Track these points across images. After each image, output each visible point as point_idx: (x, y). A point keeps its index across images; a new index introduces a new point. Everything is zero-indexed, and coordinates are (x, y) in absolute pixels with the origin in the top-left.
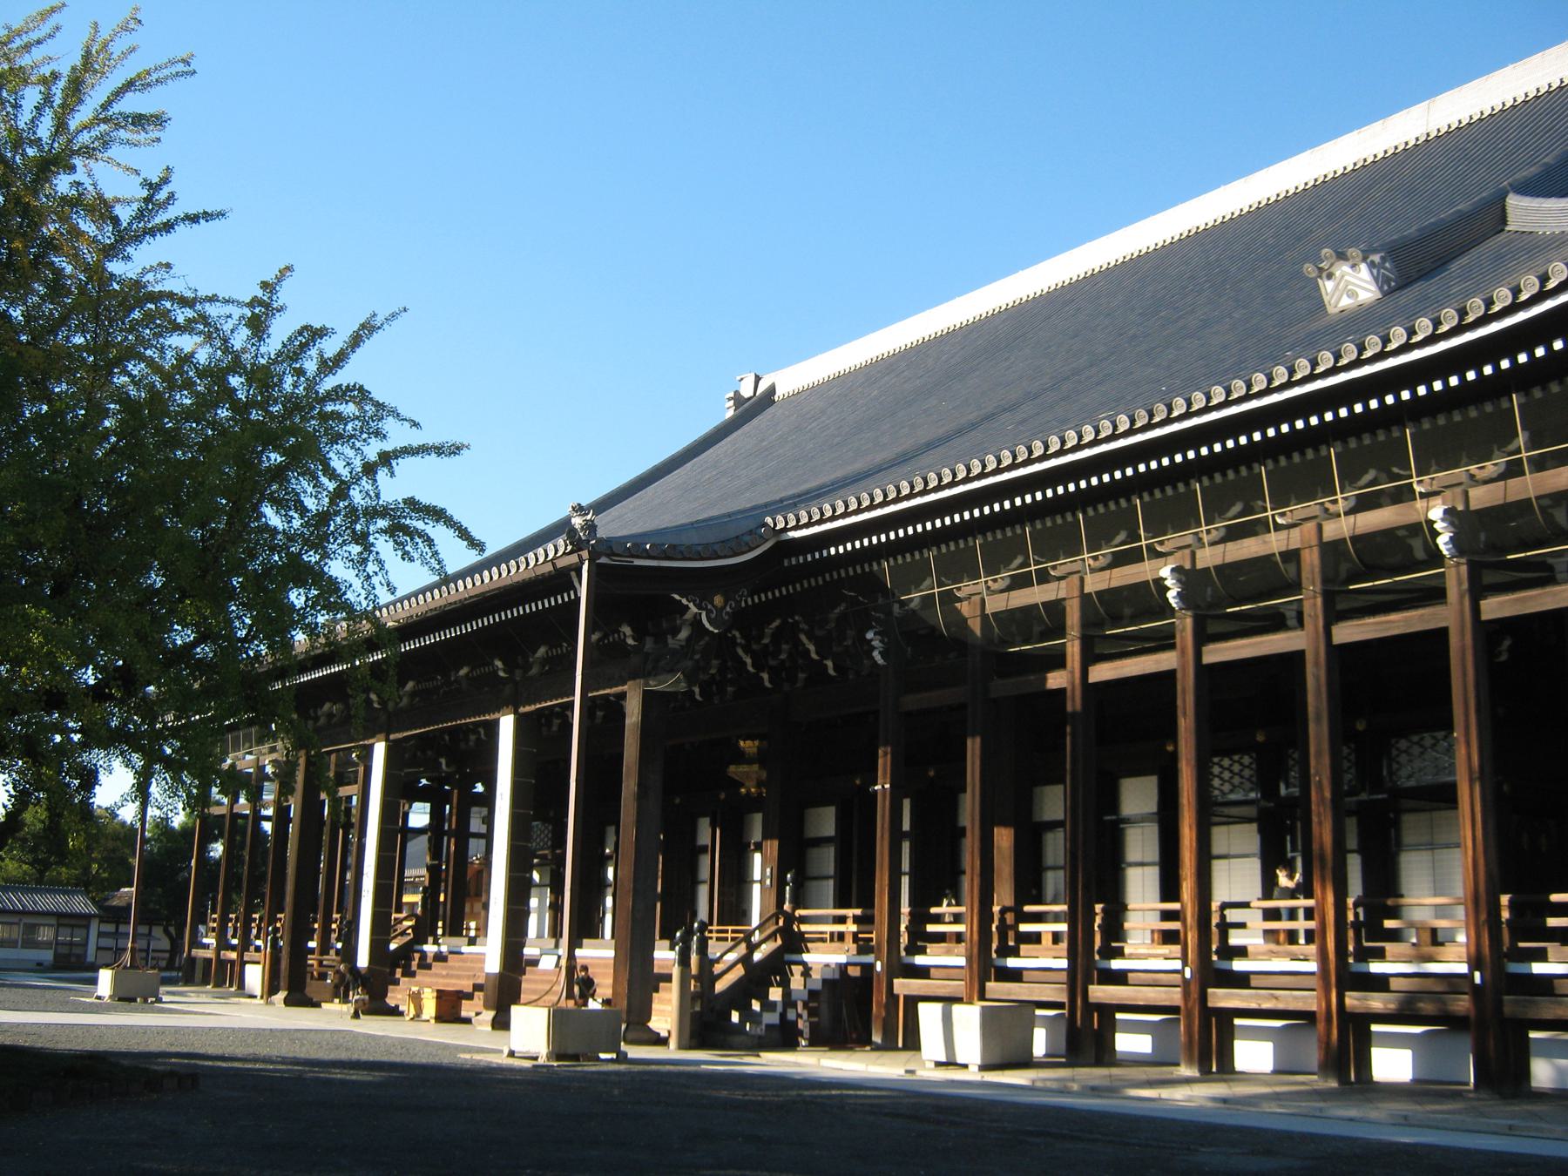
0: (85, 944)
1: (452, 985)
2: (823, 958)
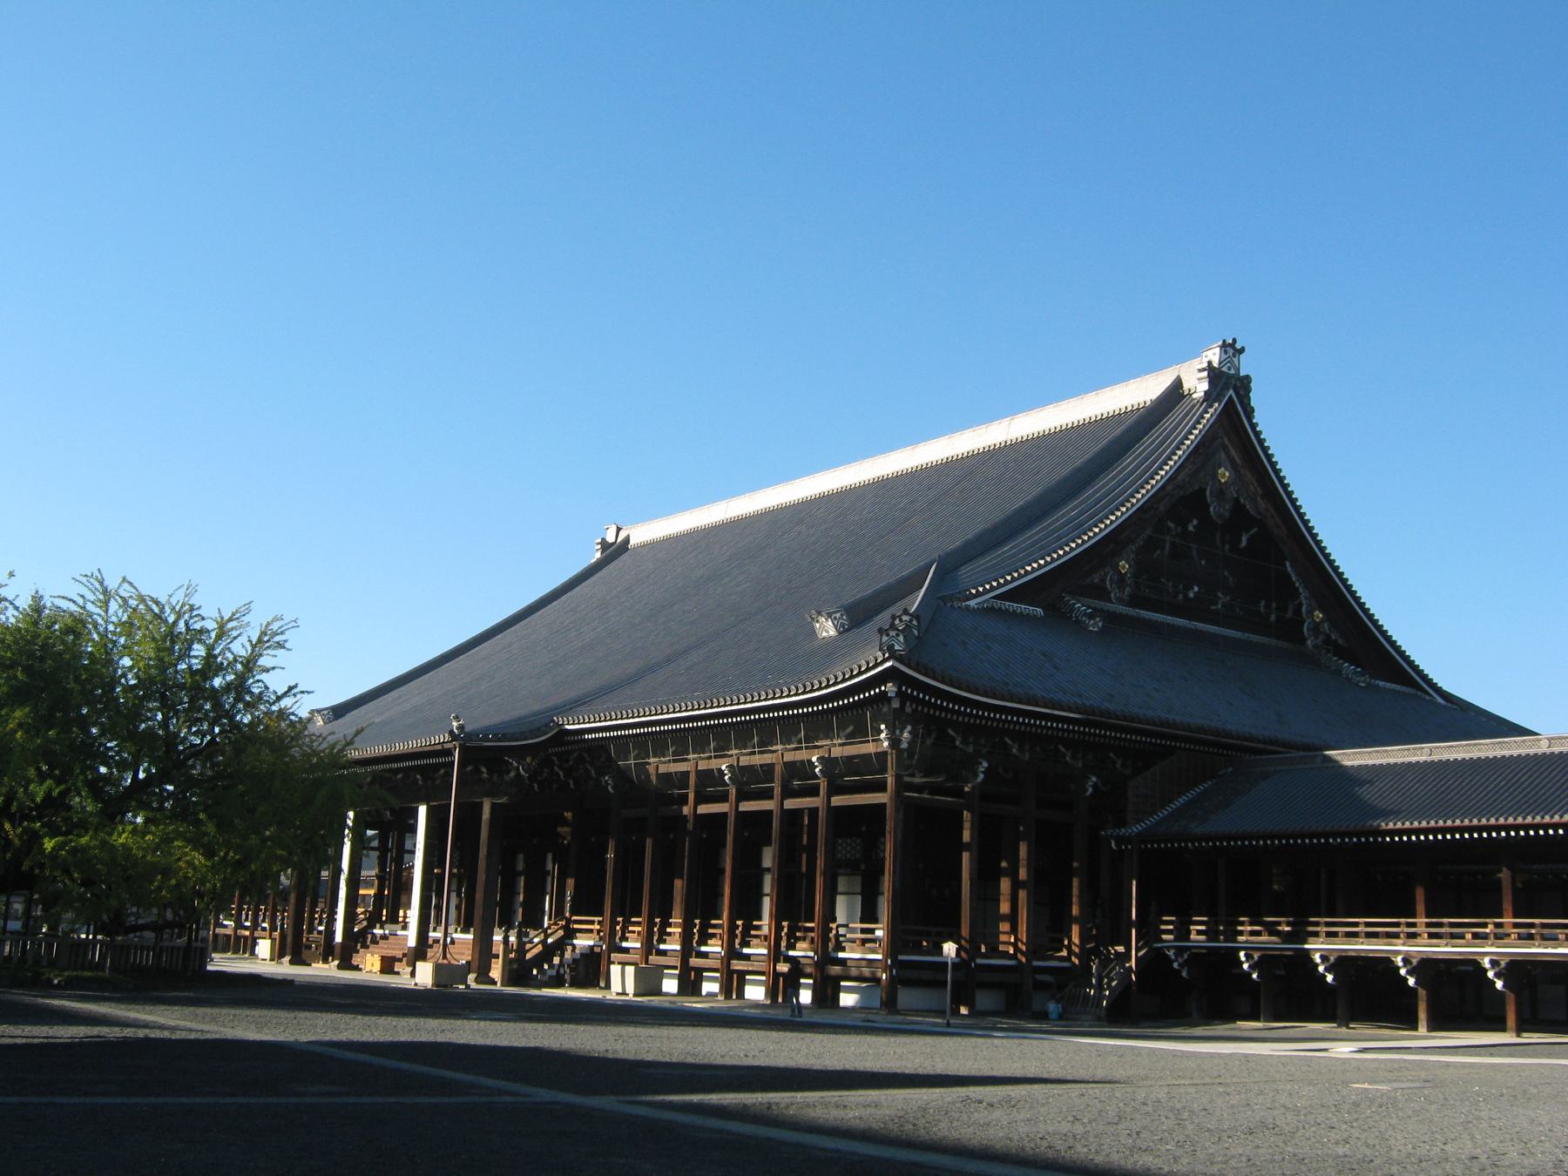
1: (390, 953)
2: (583, 942)
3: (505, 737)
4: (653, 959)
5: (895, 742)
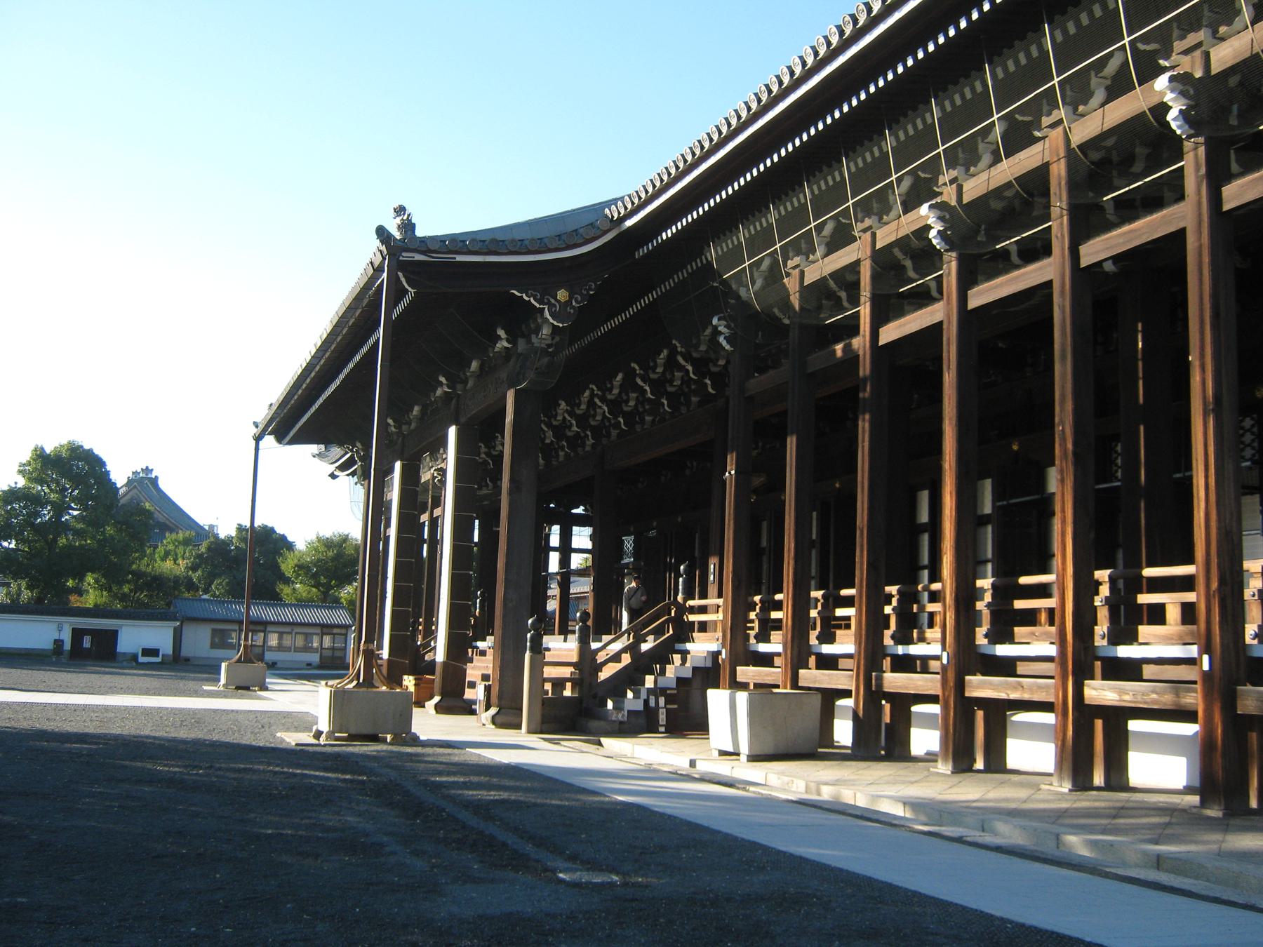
0: (345, 649)
4: (812, 676)
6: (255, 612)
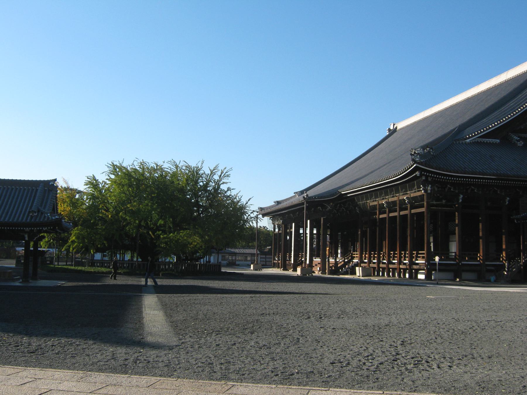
3: (321, 197)
5: (426, 191)
6: (233, 250)
